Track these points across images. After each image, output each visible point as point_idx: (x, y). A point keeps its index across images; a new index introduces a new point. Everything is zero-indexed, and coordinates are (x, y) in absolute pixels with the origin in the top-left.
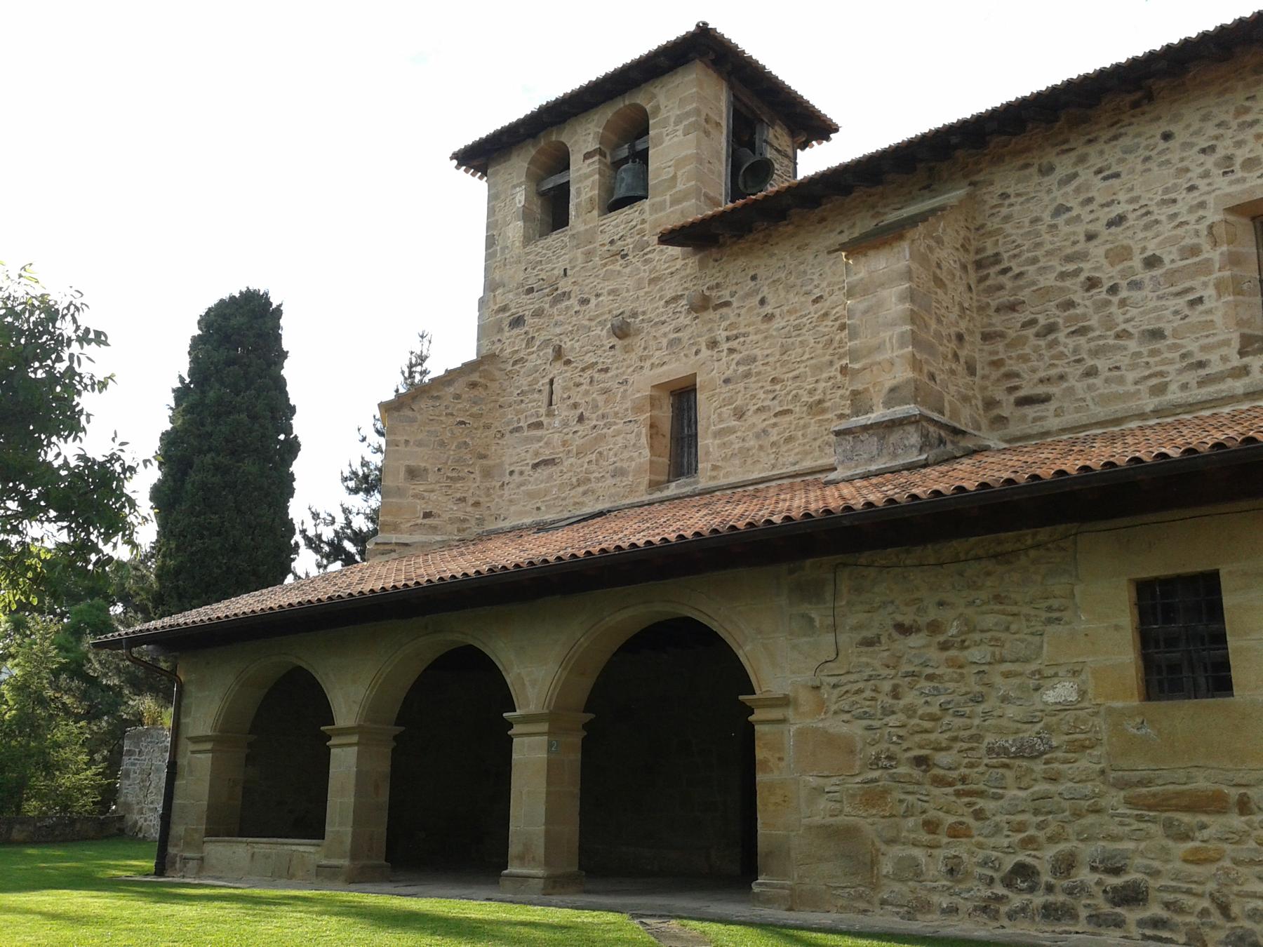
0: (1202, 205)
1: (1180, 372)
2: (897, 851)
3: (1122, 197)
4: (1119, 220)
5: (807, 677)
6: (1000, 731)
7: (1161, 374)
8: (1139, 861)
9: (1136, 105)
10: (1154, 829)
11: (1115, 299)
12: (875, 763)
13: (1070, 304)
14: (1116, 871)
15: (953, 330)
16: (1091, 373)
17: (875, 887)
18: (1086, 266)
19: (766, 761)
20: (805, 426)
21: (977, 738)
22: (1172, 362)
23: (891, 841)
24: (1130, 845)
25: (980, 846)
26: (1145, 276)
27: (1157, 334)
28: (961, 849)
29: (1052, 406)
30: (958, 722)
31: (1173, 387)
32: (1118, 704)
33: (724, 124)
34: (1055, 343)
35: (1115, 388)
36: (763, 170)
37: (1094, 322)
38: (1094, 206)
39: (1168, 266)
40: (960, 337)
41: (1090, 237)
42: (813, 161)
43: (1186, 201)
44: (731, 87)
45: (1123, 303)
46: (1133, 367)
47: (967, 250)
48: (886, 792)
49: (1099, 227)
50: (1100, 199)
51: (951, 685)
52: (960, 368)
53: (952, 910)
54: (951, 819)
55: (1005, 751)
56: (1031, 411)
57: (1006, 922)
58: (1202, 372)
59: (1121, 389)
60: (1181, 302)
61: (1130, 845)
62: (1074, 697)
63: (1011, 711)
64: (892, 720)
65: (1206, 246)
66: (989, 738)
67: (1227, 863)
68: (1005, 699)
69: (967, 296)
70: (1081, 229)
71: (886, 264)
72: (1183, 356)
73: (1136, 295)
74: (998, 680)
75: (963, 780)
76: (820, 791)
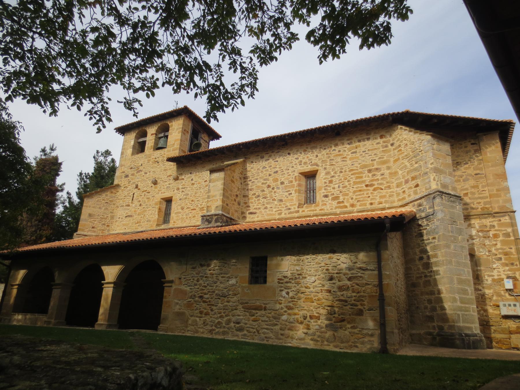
0: (294, 171)
1: (285, 210)
2: (193, 318)
3: (278, 166)
4: (276, 172)
5: (178, 276)
6: (219, 290)
7: (281, 210)
8: (243, 321)
9: (283, 145)
10: (247, 314)
11: (273, 191)
12: (191, 297)
13: (263, 191)
14: (238, 323)
15: (235, 194)
16: (266, 208)
17: (187, 327)
18: (268, 182)
19: (166, 296)
20: (198, 214)
21: (214, 292)
22: (283, 208)
23: (191, 316)
24: (242, 317)
25: (211, 317)
26: (280, 186)
27: (281, 201)
28: (207, 318)
29: (257, 215)
30: (210, 288)
31: (283, 214)
32: (244, 285)
33: (190, 132)
34: (259, 200)
35: (271, 212)
36: (199, 145)
37: (268, 196)
38: (271, 168)
39: (285, 184)
40: (237, 196)
41: (270, 175)
42: (214, 145)
43: (291, 169)
44: (193, 122)
45: (275, 192)
46: (275, 208)
47: (242, 174)
48: (193, 304)
49: (272, 173)
50: (273, 166)
51: (210, 279)
52: (236, 203)
53: (203, 333)
54: (206, 311)
55: (219, 295)
56: (252, 216)
57: (214, 335)
58: (290, 211)
59: (272, 213)
60: (287, 194)
61: (242, 317)
62: (235, 283)
63: (222, 285)
64: (196, 287)
65: (294, 181)
66: (216, 292)
67: (260, 321)
68: (221, 283)
69: (240, 185)
70: (268, 173)
71: (220, 175)
72: (286, 206)
73: (278, 191)
74: (220, 278)
75: (210, 301)
76: (177, 303)
